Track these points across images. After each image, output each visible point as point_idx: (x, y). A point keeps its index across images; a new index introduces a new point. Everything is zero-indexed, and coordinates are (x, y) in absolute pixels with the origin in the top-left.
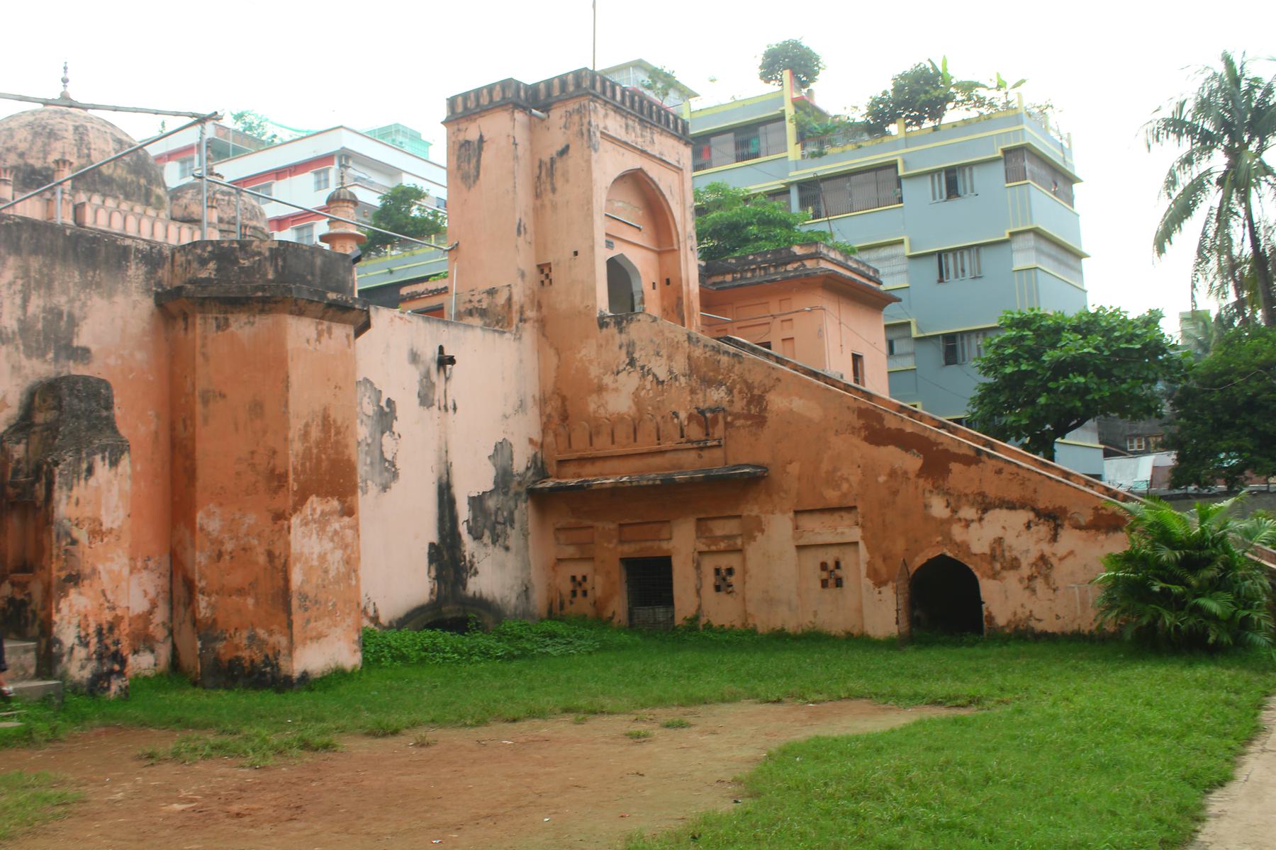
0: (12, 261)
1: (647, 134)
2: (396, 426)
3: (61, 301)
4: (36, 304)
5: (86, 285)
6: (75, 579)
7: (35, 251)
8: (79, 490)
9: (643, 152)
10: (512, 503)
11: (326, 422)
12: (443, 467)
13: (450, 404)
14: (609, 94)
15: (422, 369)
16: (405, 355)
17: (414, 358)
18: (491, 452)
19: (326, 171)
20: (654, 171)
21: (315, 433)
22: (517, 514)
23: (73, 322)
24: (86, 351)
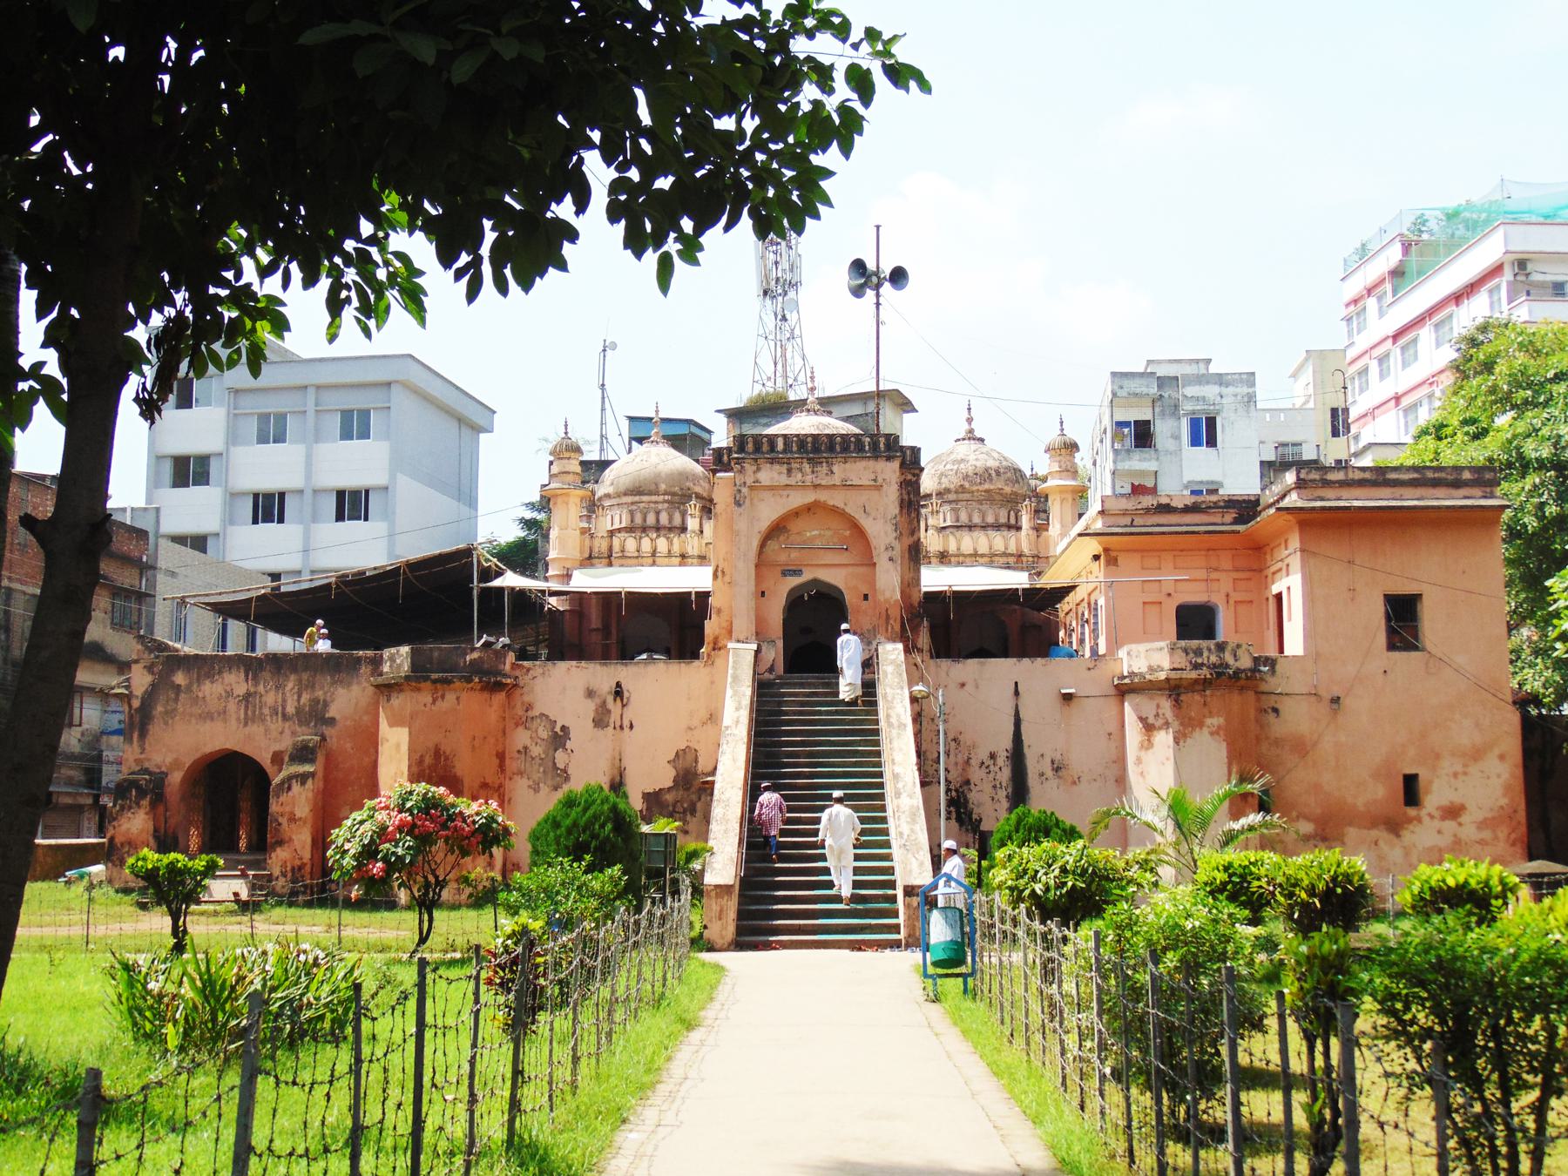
0: (292, 677)
1: (824, 469)
2: (569, 745)
3: (320, 694)
4: (305, 698)
5: (334, 683)
6: (280, 843)
7: (306, 669)
8: (283, 798)
9: (816, 486)
10: (694, 797)
11: (437, 753)
12: (616, 772)
13: (626, 723)
14: (765, 448)
15: (598, 701)
16: (581, 692)
17: (590, 693)
18: (672, 756)
19: (1498, 287)
20: (836, 499)
21: (428, 760)
22: (699, 805)
23: (326, 704)
24: (333, 719)
